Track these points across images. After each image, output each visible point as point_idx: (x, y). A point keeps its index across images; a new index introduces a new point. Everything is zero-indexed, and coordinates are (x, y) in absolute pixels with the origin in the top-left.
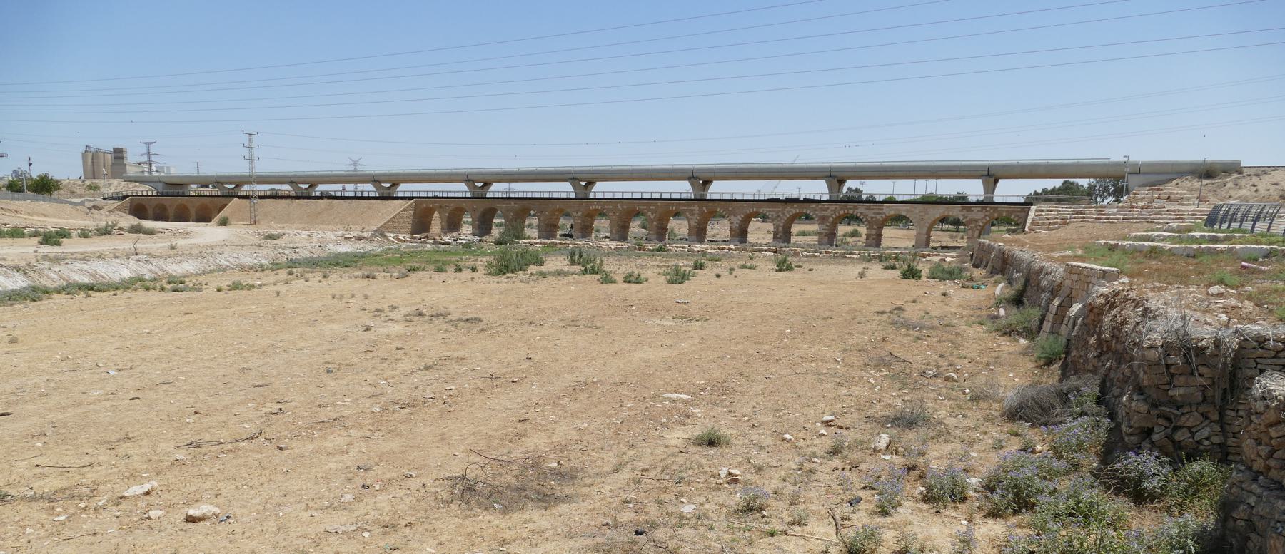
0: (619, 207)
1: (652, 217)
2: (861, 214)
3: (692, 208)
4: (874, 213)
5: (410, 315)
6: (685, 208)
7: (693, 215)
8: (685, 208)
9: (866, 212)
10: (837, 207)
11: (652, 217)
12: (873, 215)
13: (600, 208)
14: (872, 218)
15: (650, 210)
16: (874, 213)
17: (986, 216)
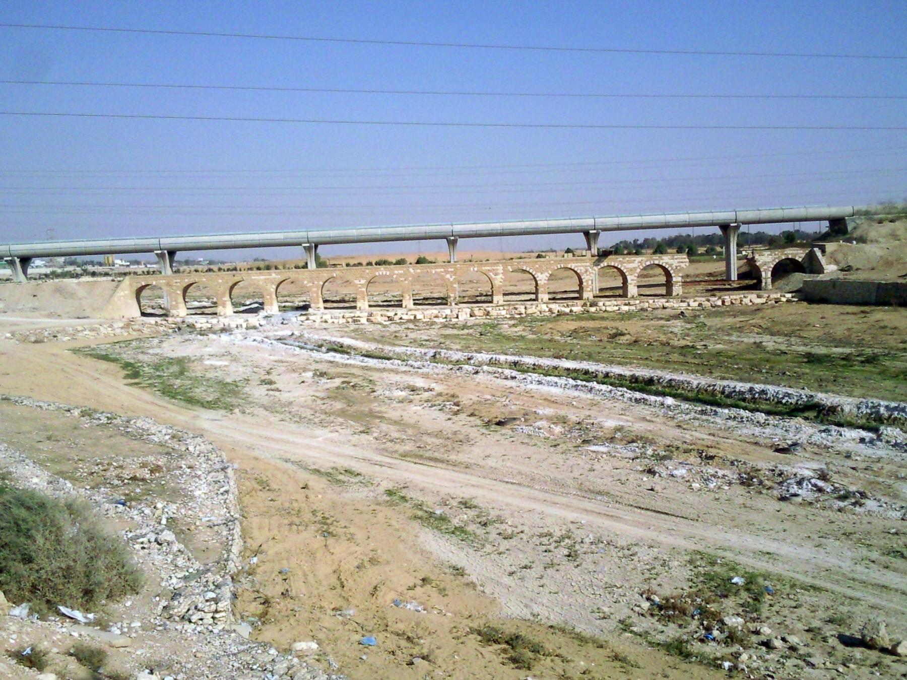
0: (412, 271)
1: (451, 280)
2: (666, 263)
3: (495, 268)
4: (679, 262)
5: (337, 469)
6: (488, 268)
7: (496, 274)
8: (488, 268)
9: (671, 261)
10: (643, 258)
11: (451, 280)
12: (678, 265)
13: (388, 273)
14: (676, 267)
15: (447, 272)
16: (679, 262)
17: (775, 259)
